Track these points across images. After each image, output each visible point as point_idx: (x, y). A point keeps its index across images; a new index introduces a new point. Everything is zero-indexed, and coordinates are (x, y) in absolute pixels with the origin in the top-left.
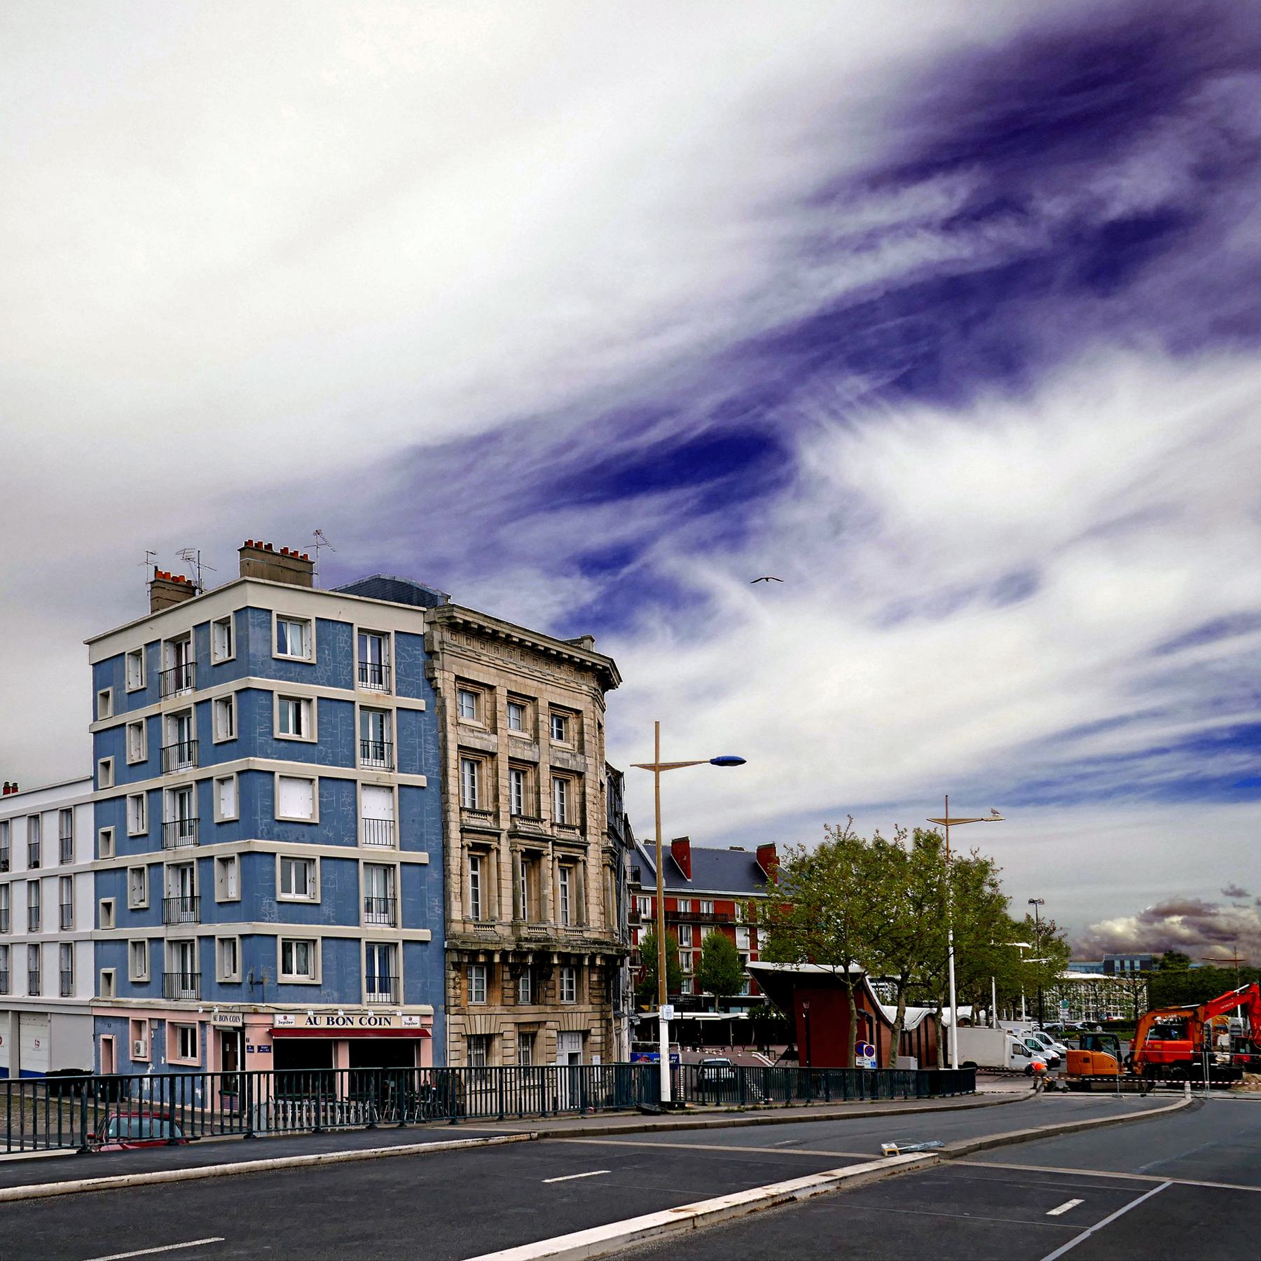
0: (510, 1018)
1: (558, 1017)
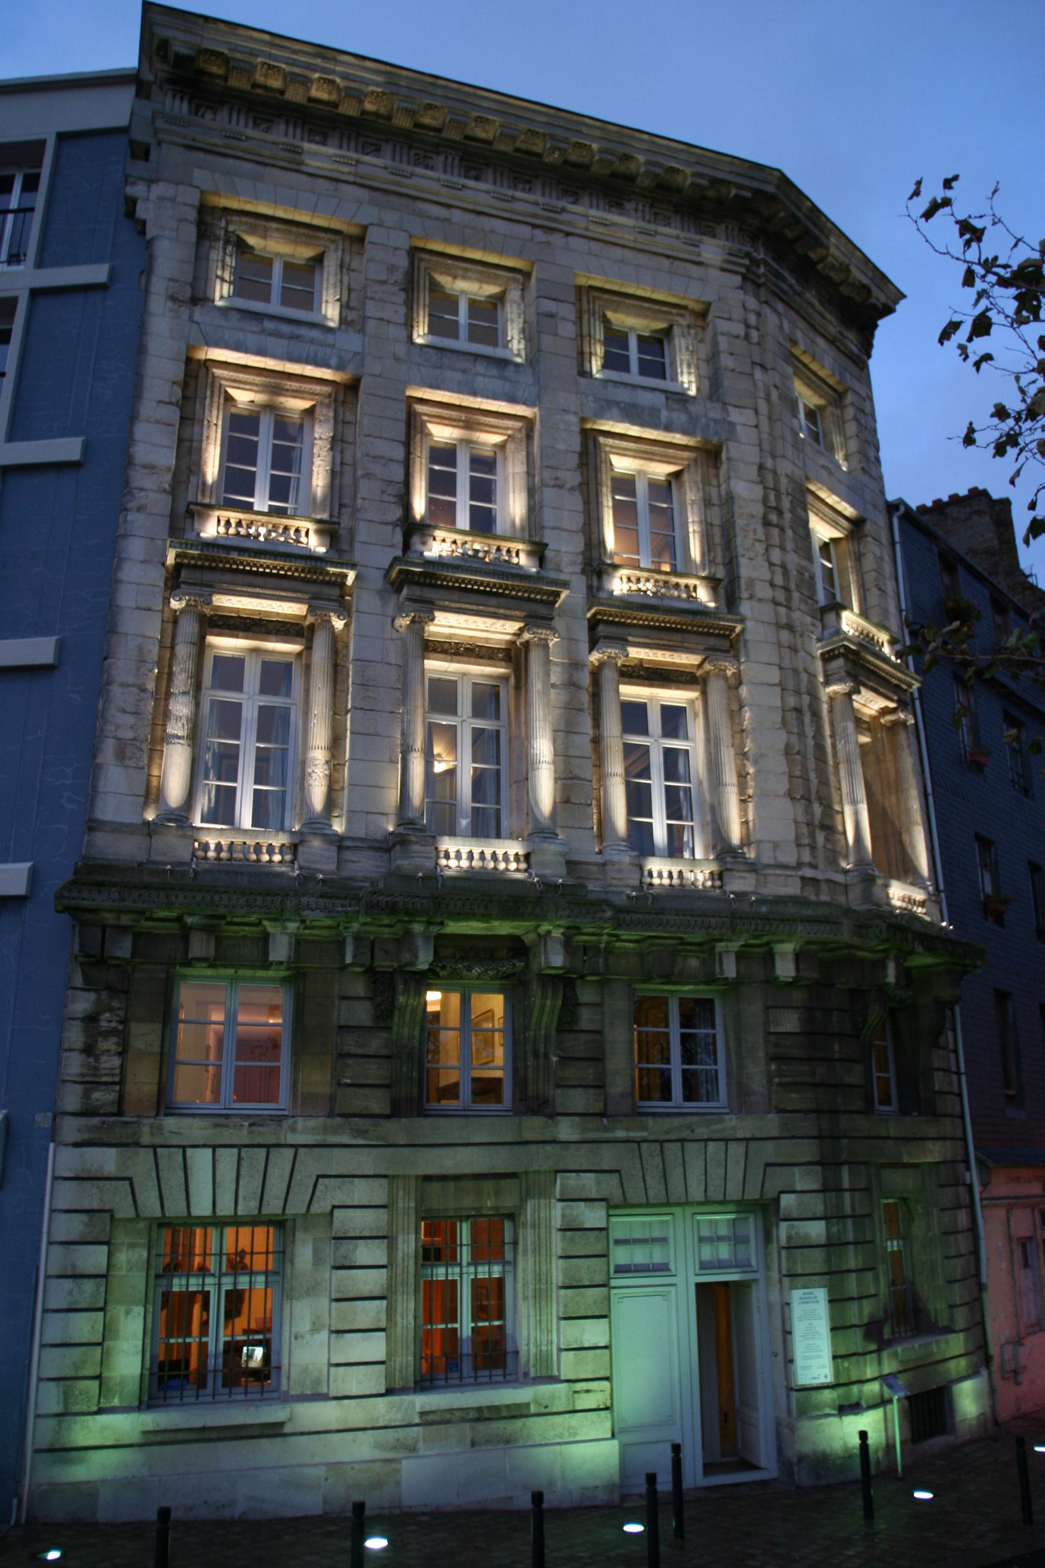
0: (365, 1161)
1: (607, 1157)
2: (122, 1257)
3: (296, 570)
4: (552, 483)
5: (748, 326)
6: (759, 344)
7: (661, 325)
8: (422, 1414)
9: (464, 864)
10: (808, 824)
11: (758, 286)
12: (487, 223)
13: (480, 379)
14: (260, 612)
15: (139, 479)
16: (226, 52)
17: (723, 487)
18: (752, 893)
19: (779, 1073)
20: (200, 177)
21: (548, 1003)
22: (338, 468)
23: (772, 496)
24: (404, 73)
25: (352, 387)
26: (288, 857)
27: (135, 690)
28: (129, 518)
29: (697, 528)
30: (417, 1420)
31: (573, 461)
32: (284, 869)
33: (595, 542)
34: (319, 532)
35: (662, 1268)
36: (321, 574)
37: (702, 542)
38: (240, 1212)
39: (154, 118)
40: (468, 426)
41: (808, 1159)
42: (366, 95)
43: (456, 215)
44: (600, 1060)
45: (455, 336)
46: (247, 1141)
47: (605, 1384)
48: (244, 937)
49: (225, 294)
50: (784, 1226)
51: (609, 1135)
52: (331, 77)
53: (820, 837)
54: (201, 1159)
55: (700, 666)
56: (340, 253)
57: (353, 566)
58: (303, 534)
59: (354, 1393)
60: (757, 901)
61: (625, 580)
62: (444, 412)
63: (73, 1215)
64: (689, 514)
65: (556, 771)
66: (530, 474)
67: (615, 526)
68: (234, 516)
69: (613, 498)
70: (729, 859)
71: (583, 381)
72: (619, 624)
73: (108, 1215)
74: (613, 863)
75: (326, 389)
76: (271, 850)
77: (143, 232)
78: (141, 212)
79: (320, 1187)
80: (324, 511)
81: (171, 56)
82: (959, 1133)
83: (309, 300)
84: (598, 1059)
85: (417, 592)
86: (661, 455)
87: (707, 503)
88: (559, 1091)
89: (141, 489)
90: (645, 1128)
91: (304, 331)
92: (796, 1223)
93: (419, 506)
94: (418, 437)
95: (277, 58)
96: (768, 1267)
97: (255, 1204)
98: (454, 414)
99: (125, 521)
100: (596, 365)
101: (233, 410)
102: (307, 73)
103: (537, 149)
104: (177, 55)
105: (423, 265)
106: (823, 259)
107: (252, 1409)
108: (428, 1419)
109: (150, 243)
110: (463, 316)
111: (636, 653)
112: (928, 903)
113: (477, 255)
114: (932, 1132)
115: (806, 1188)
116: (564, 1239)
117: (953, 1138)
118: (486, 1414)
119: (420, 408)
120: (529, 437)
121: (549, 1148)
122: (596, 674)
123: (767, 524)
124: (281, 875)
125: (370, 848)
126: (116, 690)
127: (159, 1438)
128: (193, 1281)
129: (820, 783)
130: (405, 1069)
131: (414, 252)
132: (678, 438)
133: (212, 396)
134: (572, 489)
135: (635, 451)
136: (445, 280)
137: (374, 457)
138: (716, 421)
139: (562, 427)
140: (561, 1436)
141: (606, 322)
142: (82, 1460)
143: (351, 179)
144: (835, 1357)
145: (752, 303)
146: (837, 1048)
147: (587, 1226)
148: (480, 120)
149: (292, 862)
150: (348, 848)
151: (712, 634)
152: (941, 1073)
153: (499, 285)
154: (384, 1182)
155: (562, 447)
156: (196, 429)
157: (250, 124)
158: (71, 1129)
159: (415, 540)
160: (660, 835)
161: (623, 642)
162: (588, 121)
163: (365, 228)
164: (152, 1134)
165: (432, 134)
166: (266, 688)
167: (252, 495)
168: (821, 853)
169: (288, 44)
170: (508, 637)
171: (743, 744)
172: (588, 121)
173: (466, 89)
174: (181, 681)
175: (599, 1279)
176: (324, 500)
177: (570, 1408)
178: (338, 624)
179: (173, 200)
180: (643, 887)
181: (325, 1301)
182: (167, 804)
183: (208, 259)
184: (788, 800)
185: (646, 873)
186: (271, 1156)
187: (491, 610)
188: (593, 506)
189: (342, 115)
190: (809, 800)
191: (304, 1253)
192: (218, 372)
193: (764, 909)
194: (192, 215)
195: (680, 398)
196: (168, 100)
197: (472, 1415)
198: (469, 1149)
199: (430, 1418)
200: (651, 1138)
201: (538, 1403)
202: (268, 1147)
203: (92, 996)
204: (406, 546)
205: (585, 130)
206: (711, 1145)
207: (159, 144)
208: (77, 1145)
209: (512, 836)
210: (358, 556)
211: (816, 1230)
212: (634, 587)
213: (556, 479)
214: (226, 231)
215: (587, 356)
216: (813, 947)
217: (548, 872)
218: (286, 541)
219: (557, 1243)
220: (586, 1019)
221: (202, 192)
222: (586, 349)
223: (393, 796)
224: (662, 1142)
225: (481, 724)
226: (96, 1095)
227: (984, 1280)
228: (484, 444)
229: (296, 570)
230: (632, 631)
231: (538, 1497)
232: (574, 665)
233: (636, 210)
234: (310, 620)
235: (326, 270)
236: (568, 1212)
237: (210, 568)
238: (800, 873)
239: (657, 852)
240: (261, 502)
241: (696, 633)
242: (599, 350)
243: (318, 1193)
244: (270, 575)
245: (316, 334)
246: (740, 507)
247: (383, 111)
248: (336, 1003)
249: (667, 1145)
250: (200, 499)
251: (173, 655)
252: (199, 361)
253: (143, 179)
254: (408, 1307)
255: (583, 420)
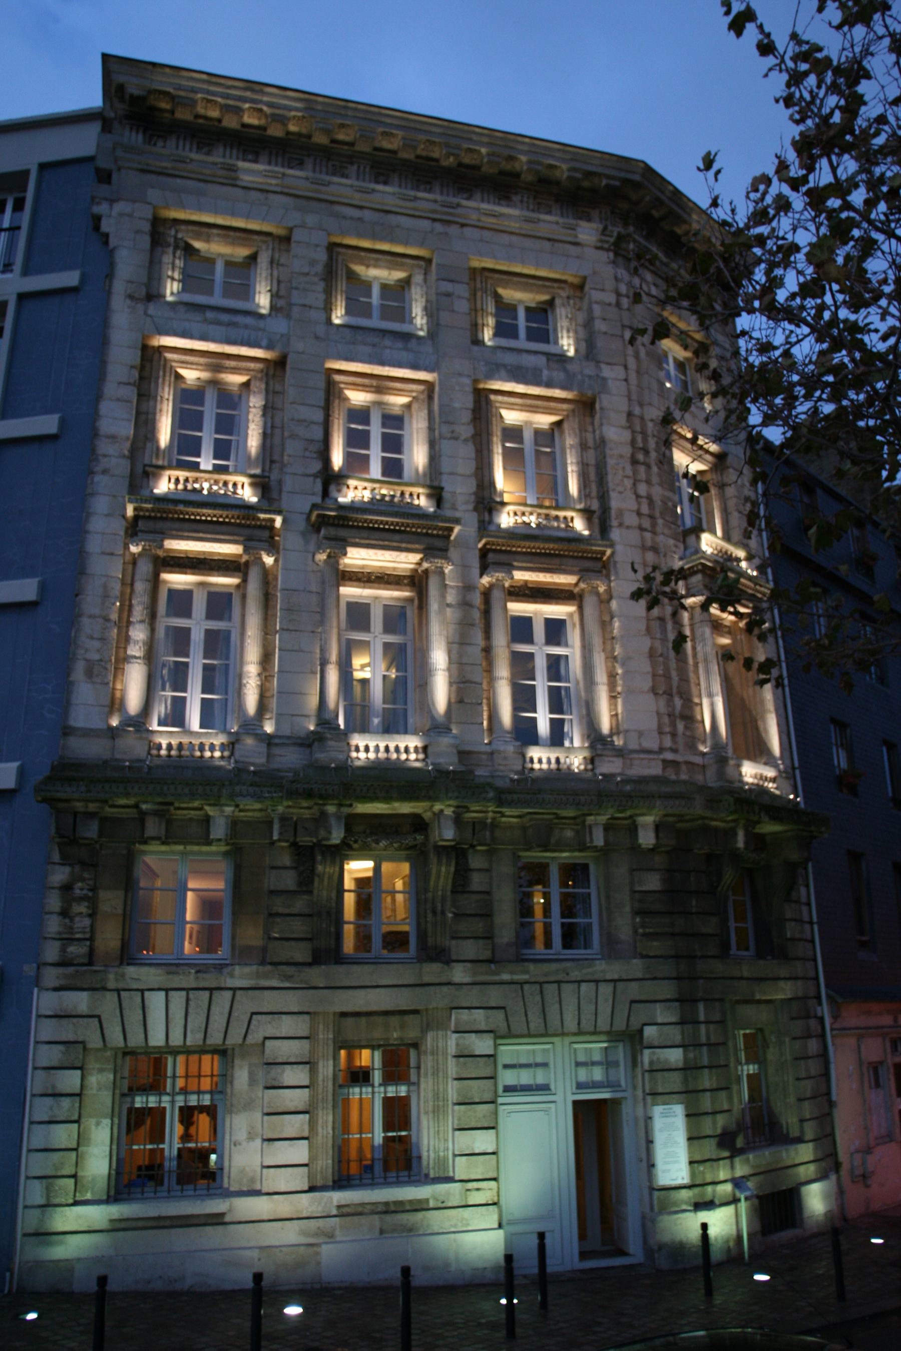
0: (292, 1001)
1: (494, 996)
2: (93, 1080)
3: (233, 517)
4: (449, 435)
5: (618, 294)
6: (628, 309)
7: (545, 297)
8: (339, 1207)
9: (372, 755)
10: (669, 715)
11: (629, 260)
12: (393, 219)
13: (388, 351)
14: (204, 553)
15: (104, 447)
16: (172, 91)
17: (597, 432)
18: (619, 774)
19: (643, 926)
20: (154, 195)
21: (443, 869)
22: (269, 431)
23: (639, 438)
24: (320, 99)
25: (280, 364)
26: (226, 754)
27: (101, 621)
29: (575, 468)
30: (334, 1212)
31: (467, 416)
32: (222, 763)
33: (486, 483)
34: (252, 485)
35: (544, 1088)
36: (253, 519)
37: (579, 480)
38: (188, 1043)
39: (114, 149)
40: (379, 390)
41: (669, 997)
42: (289, 119)
43: (367, 215)
44: (488, 915)
45: (369, 315)
46: (194, 986)
47: (493, 1184)
48: (191, 819)
49: (175, 290)
50: (647, 1052)
51: (496, 978)
52: (259, 106)
53: (680, 726)
54: (156, 1000)
55: (576, 585)
56: (270, 252)
57: (279, 513)
58: (239, 487)
59: (282, 1190)
60: (622, 781)
61: (512, 514)
62: (359, 380)
63: (53, 1046)
64: (568, 456)
65: (450, 676)
66: (431, 429)
67: (505, 468)
68: (182, 474)
69: (504, 446)
70: (599, 746)
71: (476, 348)
72: (505, 552)
73: (81, 1046)
74: (499, 752)
75: (259, 366)
76: (212, 748)
77: (106, 243)
78: (105, 227)
79: (254, 1022)
80: (257, 467)
81: (127, 97)
82: (812, 974)
83: (247, 292)
84: (486, 914)
85: (332, 532)
86: (544, 408)
87: (583, 446)
88: (454, 942)
89: (105, 456)
90: (526, 972)
91: (240, 319)
92: (658, 1050)
93: (337, 459)
94: (337, 401)
95: (213, 94)
96: (635, 1087)
97: (200, 1036)
98: (366, 381)
99: (92, 483)
100: (487, 335)
101: (183, 386)
102: (239, 104)
103: (436, 154)
104: (132, 96)
105: (340, 258)
106: (687, 233)
107: (199, 1202)
108: (344, 1212)
109: (111, 253)
110: (376, 298)
111: (520, 576)
112: (779, 780)
113: (386, 247)
114: (783, 973)
115: (666, 1020)
116: (458, 1064)
117: (804, 978)
118: (392, 1208)
119: (338, 378)
120: (430, 398)
121: (445, 989)
122: (487, 594)
123: (634, 462)
124: (219, 768)
125: (295, 744)
126: (85, 621)
127: (123, 1225)
129: (681, 680)
130: (324, 926)
131: (332, 247)
132: (558, 393)
133: (164, 375)
134: (466, 440)
135: (522, 405)
136: (359, 269)
137: (298, 421)
138: (590, 377)
139: (457, 388)
140: (455, 1226)
141: (497, 297)
142: (61, 1243)
143: (278, 189)
144: (691, 1163)
145: (622, 273)
146: (694, 903)
147: (477, 1053)
148: (385, 134)
149: (230, 757)
150: (277, 745)
151: (587, 558)
152: (793, 924)
153: (405, 271)
154: (307, 1017)
155: (457, 405)
156: (151, 403)
157: (195, 147)
158: (51, 976)
159: (332, 488)
160: (543, 727)
161: (509, 567)
162: (477, 130)
163: (291, 230)
164: (117, 980)
165: (346, 147)
166: (211, 614)
167: (199, 456)
168: (681, 740)
169: (223, 81)
170: (412, 566)
171: (613, 650)
172: (477, 130)
173: (373, 109)
174: (139, 612)
175: (488, 1096)
176: (257, 458)
177: (463, 1203)
178: (269, 560)
179: (130, 215)
180: (526, 771)
181: (258, 1115)
182: (127, 712)
183: (160, 262)
184: (651, 695)
185: (528, 760)
186: (214, 998)
187: (395, 544)
188: (485, 453)
189: (270, 137)
190: (671, 695)
191: (241, 1076)
192: (169, 356)
193: (628, 788)
194: (147, 227)
195: (561, 358)
196: (127, 133)
197: (380, 1208)
198: (378, 990)
199: (345, 1210)
200: (533, 980)
201: (436, 1200)
202: (211, 990)
203: (67, 869)
204: (325, 493)
205: (474, 137)
206: (584, 986)
207: (119, 169)
208: (56, 989)
209: (415, 733)
210: (285, 504)
211: (675, 1056)
212: (519, 521)
213: (453, 432)
214: (176, 238)
215: (480, 327)
216: (671, 819)
217: (441, 760)
218: (225, 494)
219: (452, 1067)
220: (477, 881)
221: (155, 208)
222: (480, 321)
223: (313, 701)
224: (541, 984)
225: (391, 639)
226: (71, 949)
227: (834, 1097)
228: (394, 405)
229: (233, 517)
230: (517, 557)
231: (406, 1271)
232: (468, 587)
233: (522, 201)
234: (245, 558)
235: (259, 266)
236: (461, 1041)
237: (161, 518)
238: (662, 757)
239: (540, 742)
240: (206, 462)
241: (573, 557)
242: (491, 321)
243: (252, 1027)
244: (211, 522)
245: (249, 320)
246: (611, 449)
247: (304, 131)
249: (545, 986)
250: (154, 462)
251: (132, 591)
252: (153, 347)
253: (106, 199)
254: (326, 1121)
255: (476, 381)
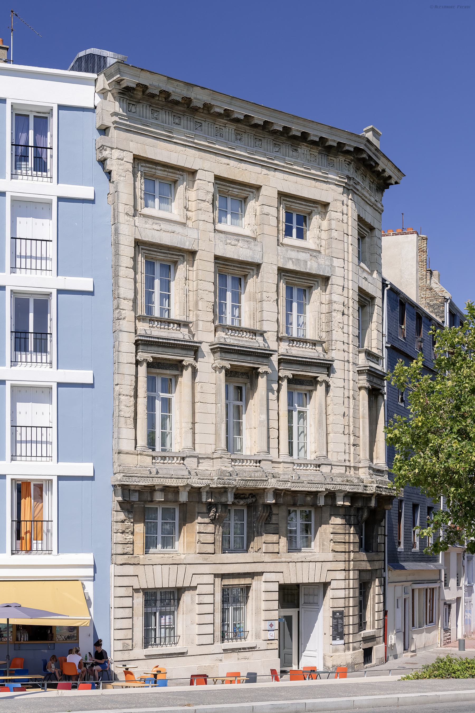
1: (279, 567)
28: (121, 323)
30: (222, 652)
128: (167, 608)
248: (197, 514)
